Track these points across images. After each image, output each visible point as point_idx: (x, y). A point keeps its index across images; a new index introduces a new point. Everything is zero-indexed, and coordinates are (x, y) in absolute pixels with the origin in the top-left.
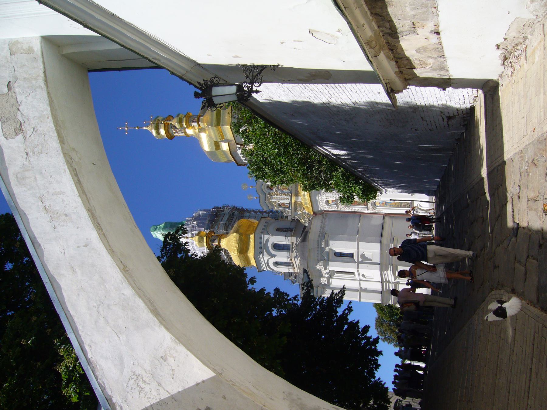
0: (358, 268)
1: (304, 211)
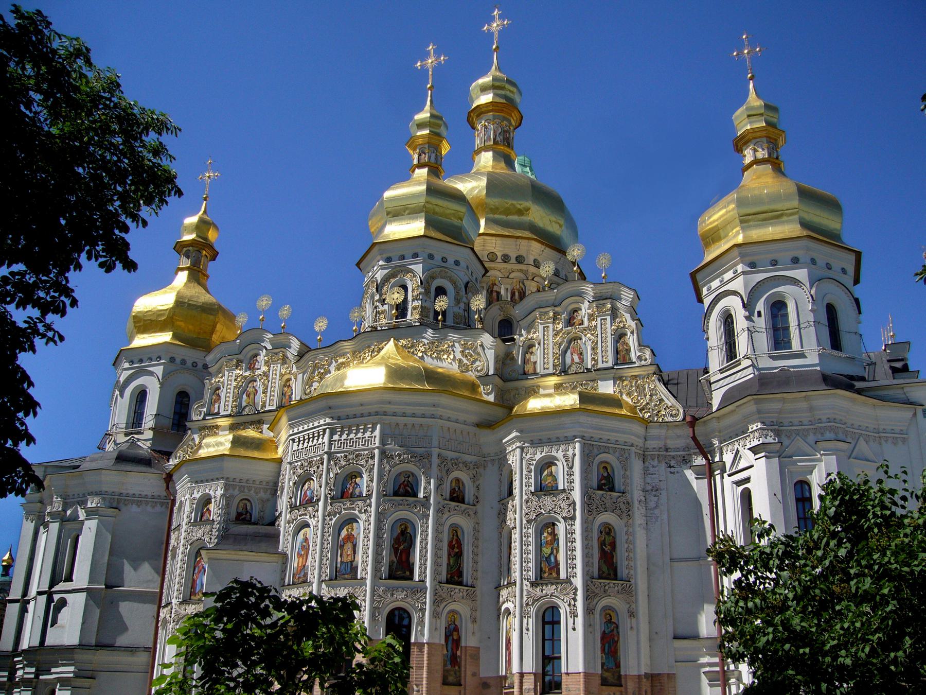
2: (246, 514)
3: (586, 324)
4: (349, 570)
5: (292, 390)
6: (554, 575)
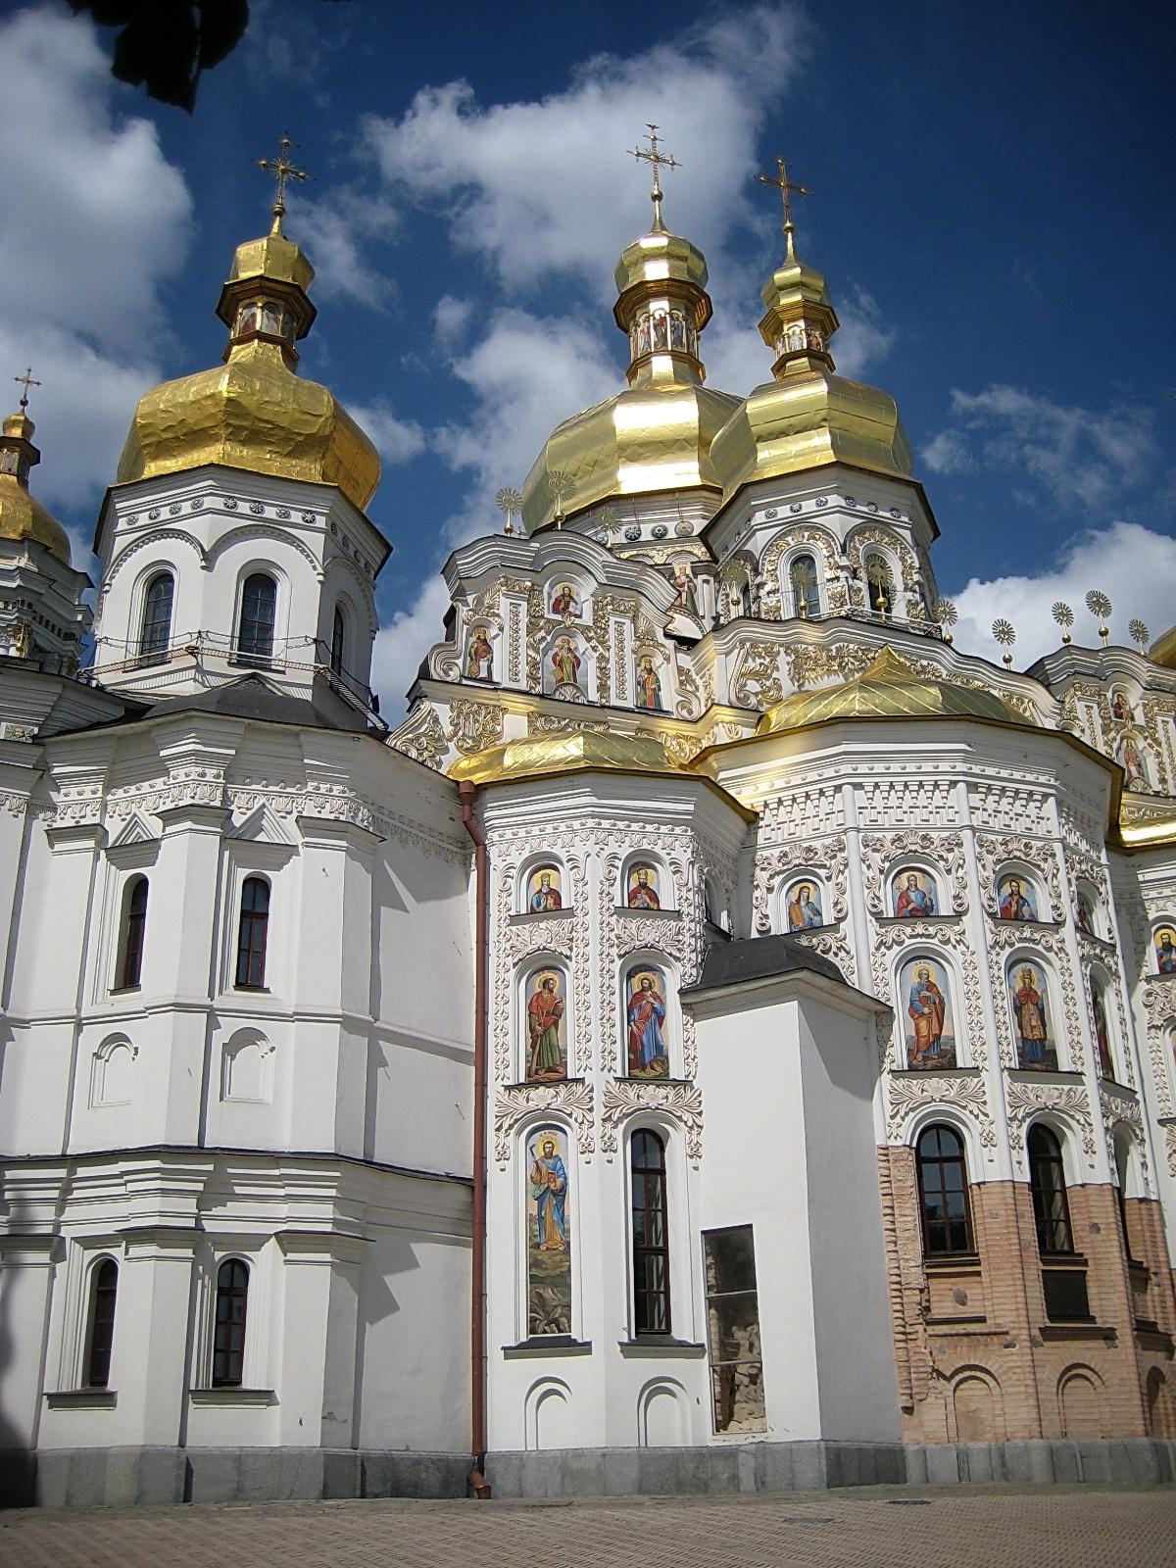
1: (451, 745)
4: (1040, 1055)
5: (658, 680)
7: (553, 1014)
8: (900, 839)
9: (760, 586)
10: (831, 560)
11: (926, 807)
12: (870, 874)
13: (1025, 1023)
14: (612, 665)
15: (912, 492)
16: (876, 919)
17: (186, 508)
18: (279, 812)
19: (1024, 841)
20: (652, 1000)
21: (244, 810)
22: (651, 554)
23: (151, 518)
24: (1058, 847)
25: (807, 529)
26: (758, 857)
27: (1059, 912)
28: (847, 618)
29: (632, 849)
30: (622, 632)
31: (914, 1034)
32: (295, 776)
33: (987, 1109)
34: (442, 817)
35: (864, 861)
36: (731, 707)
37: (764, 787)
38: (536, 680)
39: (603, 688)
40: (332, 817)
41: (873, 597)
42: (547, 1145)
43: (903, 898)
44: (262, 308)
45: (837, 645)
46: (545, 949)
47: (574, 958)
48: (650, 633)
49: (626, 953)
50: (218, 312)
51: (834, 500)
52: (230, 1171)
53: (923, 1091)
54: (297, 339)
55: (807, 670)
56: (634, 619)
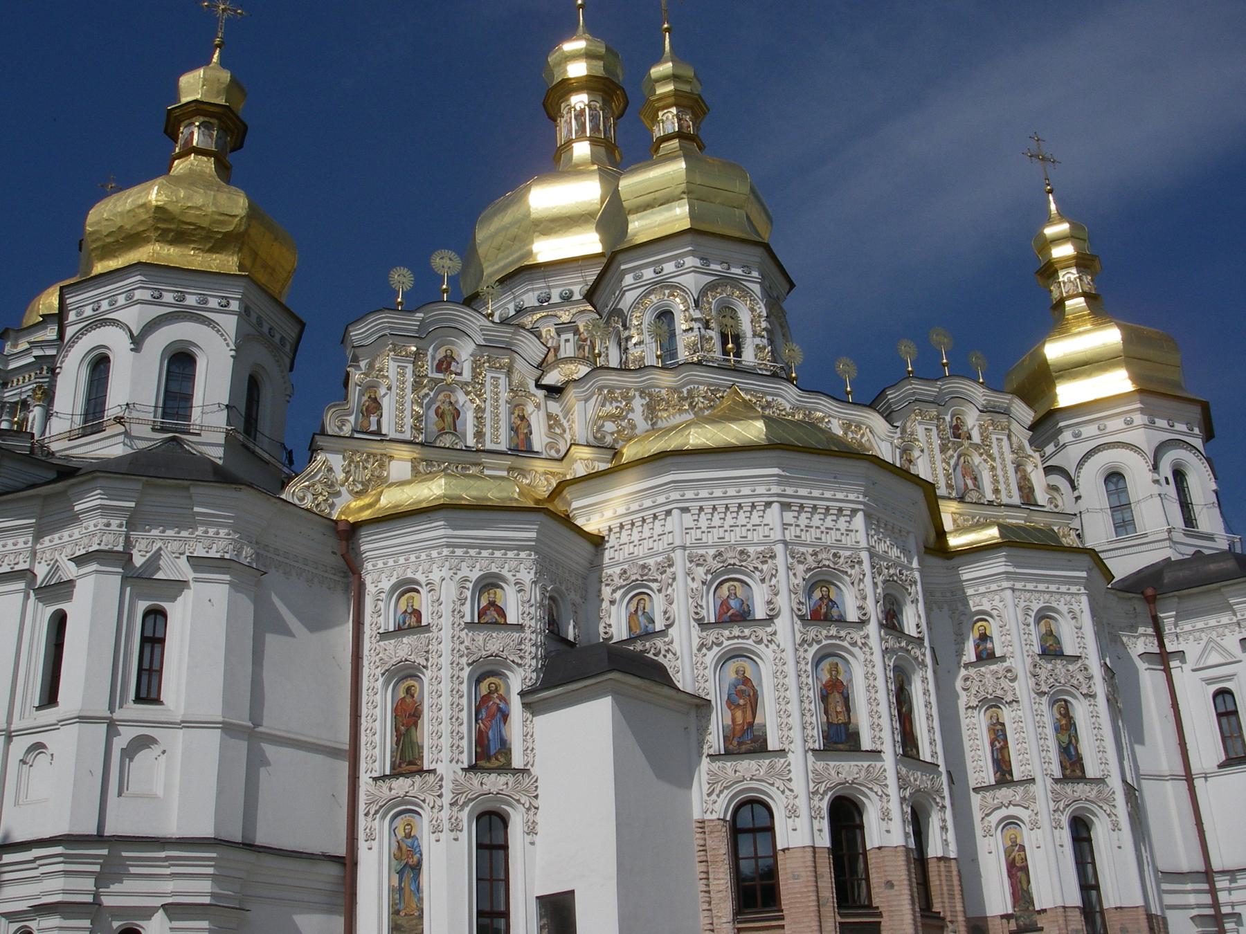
0: (83, 719)
1: (343, 490)
2: (553, 625)
3: (976, 438)
4: (844, 738)
5: (529, 425)
6: (1078, 773)
7: (414, 715)
8: (720, 554)
9: (629, 338)
10: (687, 314)
11: (745, 526)
12: (694, 585)
13: (831, 707)
14: (487, 415)
15: (760, 251)
16: (699, 624)
17: (121, 300)
18: (174, 553)
19: (833, 551)
20: (498, 701)
21: (144, 553)
22: (559, 314)
23: (94, 310)
24: (864, 556)
25: (667, 287)
26: (604, 575)
27: (863, 612)
28: (699, 363)
29: (482, 573)
30: (497, 388)
31: (730, 723)
32: (188, 522)
33: (793, 785)
34: (326, 551)
35: (689, 575)
36: (588, 445)
37: (609, 513)
38: (419, 430)
39: (479, 435)
40: (218, 556)
41: (724, 342)
42: (407, 827)
43: (724, 605)
44: (199, 127)
45: (688, 387)
46: (406, 660)
47: (430, 668)
48: (522, 384)
49: (474, 662)
50: (166, 131)
51: (690, 261)
52: (124, 854)
53: (736, 771)
54: (231, 151)
55: (660, 410)
56: (509, 373)
